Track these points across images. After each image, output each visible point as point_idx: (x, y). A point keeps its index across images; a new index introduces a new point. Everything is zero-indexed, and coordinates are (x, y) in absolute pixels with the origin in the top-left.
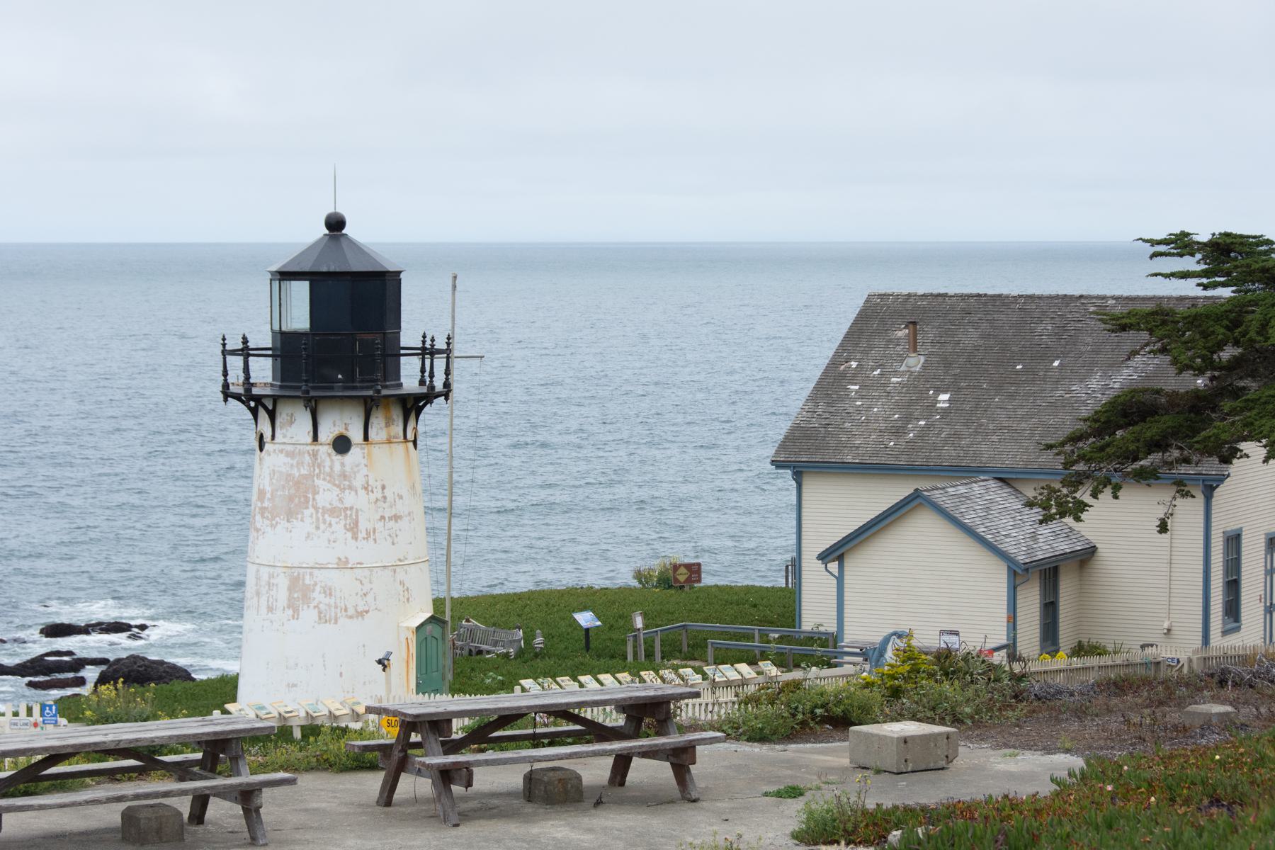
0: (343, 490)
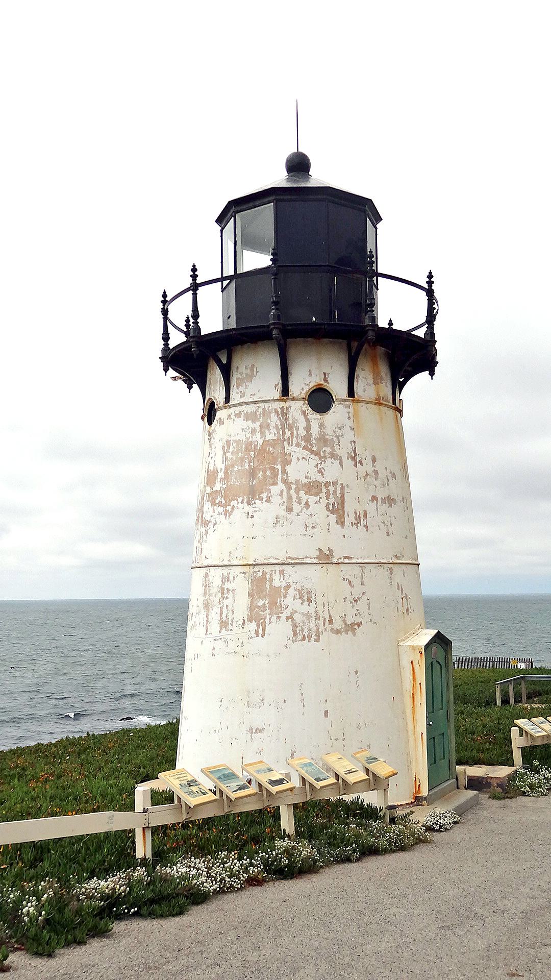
0: (323, 459)
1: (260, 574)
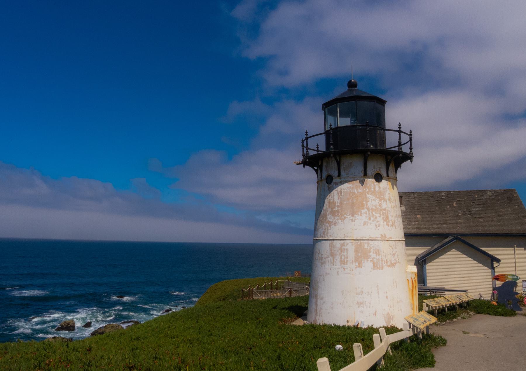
1: (359, 243)
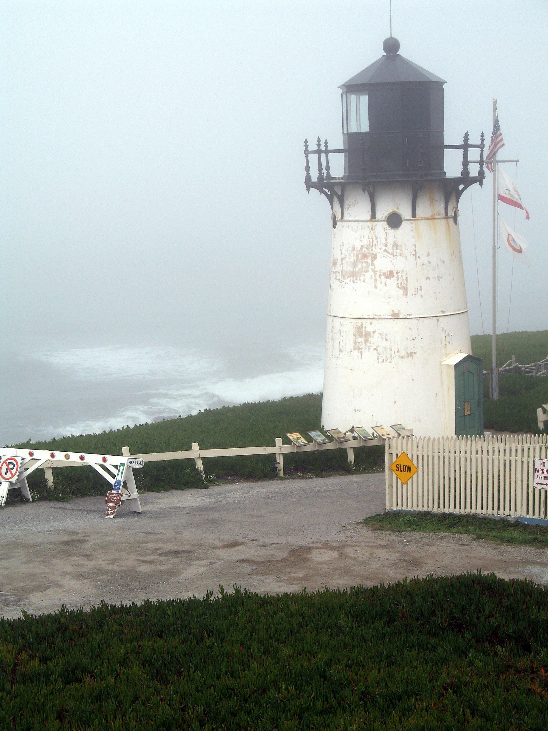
1: (359, 324)
